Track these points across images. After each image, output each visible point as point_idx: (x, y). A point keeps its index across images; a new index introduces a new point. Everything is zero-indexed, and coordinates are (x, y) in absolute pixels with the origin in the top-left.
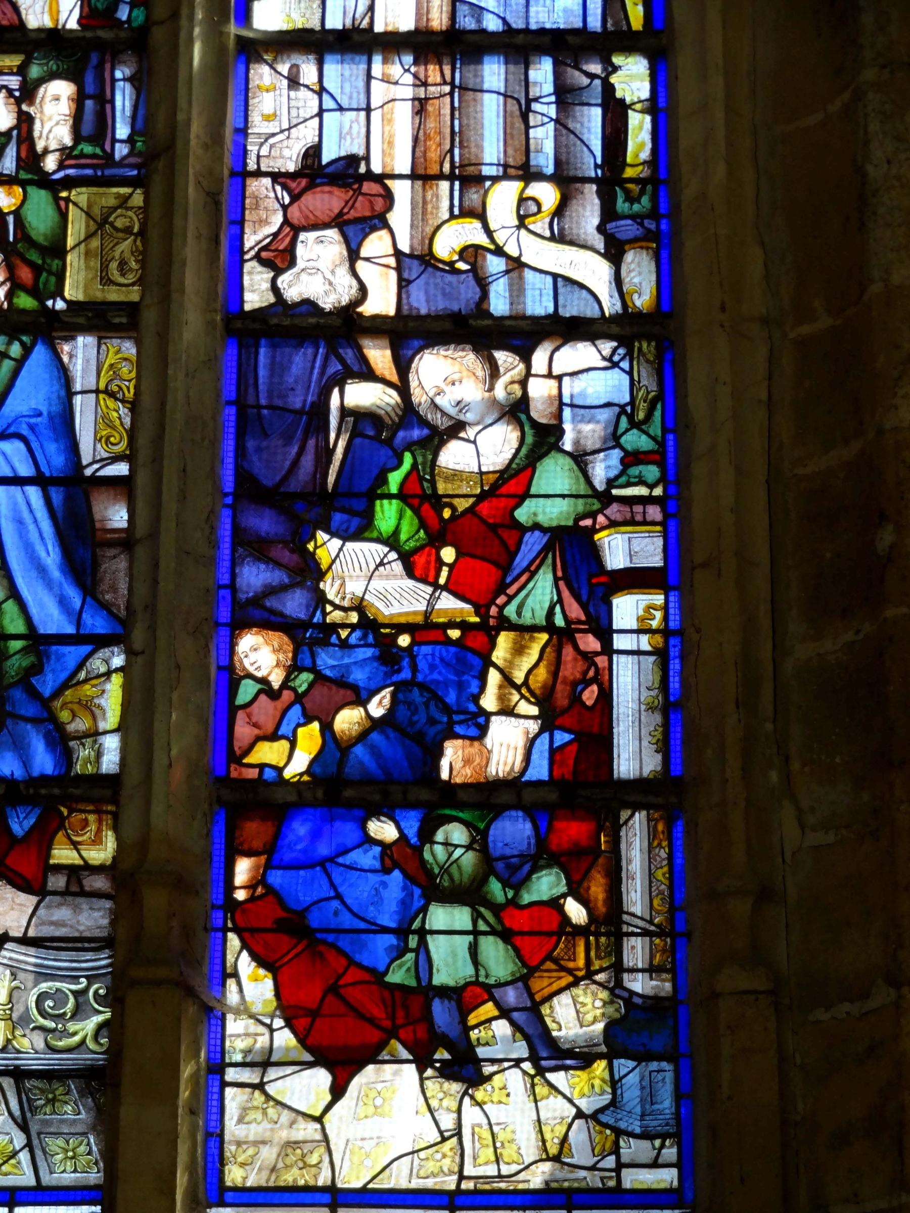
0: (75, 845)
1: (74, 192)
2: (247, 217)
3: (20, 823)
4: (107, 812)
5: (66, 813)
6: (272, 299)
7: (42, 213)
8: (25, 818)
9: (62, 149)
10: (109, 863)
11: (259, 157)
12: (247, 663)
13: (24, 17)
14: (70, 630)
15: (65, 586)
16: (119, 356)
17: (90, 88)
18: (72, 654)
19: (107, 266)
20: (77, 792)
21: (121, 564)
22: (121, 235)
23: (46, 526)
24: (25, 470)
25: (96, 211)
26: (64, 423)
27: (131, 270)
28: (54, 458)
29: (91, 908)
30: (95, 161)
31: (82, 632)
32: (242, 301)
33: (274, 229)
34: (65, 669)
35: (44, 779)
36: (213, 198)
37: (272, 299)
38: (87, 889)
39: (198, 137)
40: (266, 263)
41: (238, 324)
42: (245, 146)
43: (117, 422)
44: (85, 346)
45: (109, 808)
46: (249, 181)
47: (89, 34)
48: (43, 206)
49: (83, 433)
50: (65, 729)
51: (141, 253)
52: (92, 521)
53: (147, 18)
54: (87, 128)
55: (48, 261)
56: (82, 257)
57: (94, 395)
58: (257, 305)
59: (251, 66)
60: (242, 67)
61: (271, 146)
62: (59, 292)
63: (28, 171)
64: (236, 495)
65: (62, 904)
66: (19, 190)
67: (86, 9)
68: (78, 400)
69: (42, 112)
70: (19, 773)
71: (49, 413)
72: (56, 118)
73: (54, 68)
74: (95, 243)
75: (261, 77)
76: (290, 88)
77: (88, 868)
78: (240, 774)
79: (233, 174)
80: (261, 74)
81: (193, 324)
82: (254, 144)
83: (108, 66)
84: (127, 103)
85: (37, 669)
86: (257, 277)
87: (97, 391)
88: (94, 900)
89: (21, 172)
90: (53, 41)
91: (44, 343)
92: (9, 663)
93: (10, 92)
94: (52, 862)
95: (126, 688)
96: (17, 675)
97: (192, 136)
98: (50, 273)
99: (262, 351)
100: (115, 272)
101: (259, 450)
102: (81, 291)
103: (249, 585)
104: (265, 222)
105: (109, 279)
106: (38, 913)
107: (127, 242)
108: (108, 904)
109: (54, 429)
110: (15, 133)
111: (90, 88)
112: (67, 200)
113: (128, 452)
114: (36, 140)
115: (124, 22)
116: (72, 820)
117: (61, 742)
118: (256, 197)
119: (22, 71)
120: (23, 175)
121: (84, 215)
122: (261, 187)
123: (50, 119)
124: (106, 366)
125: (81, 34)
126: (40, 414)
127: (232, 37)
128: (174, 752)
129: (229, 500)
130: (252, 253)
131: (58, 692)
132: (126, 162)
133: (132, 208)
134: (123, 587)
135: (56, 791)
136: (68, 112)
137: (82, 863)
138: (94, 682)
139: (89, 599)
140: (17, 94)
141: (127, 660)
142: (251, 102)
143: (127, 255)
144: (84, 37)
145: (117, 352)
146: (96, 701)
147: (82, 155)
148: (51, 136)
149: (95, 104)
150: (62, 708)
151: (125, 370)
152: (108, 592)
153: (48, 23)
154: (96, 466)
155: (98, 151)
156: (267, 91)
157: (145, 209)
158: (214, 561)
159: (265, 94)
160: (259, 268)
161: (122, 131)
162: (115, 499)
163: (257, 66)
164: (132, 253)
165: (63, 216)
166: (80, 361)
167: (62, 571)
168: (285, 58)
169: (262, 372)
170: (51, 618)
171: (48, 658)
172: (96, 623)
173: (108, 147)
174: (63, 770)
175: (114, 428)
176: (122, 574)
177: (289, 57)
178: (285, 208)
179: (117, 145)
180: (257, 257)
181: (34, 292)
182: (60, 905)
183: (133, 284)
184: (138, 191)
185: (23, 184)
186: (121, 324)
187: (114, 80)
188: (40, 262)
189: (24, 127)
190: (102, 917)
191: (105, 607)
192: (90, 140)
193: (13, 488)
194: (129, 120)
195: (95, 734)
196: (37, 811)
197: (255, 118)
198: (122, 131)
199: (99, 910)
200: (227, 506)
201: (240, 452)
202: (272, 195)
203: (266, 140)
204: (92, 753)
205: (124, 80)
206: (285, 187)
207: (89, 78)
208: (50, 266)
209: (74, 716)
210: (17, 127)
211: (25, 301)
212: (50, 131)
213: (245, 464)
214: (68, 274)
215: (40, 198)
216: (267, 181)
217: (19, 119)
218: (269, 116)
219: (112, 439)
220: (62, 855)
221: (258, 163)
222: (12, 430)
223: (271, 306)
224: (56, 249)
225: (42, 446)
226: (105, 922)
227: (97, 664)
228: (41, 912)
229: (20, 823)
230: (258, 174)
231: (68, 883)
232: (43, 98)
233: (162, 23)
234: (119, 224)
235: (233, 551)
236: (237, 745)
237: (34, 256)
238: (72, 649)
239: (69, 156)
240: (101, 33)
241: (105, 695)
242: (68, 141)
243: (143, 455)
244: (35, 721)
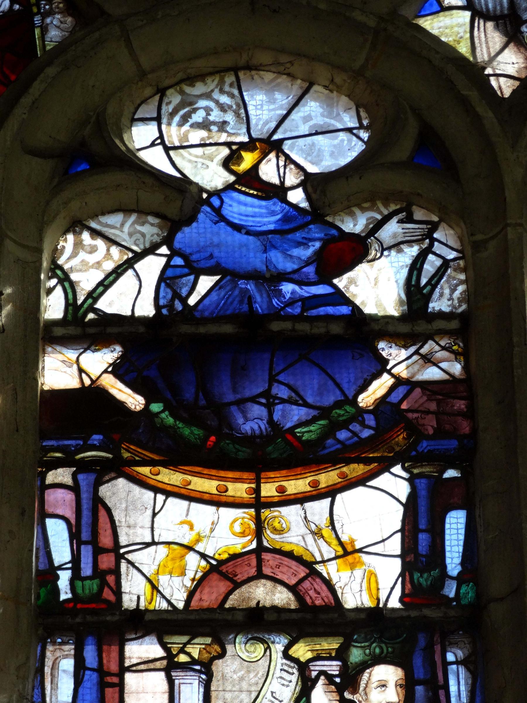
13: (340, 595)
17: (420, 673)
47: (414, 614)
53: (478, 595)
67: (408, 586)
73: (377, 651)
83: (438, 648)
84: (463, 688)
90: (373, 620)
93: (330, 678)
111: (420, 673)
115: (453, 600)
119: (341, 655)
125: (405, 614)
140: (338, 680)
144: (409, 617)
149: (427, 690)
153: (369, 603)
187: (446, 664)
205: (457, 663)
207: (418, 661)
232: (367, 685)
233: (502, 599)
240: (427, 612)
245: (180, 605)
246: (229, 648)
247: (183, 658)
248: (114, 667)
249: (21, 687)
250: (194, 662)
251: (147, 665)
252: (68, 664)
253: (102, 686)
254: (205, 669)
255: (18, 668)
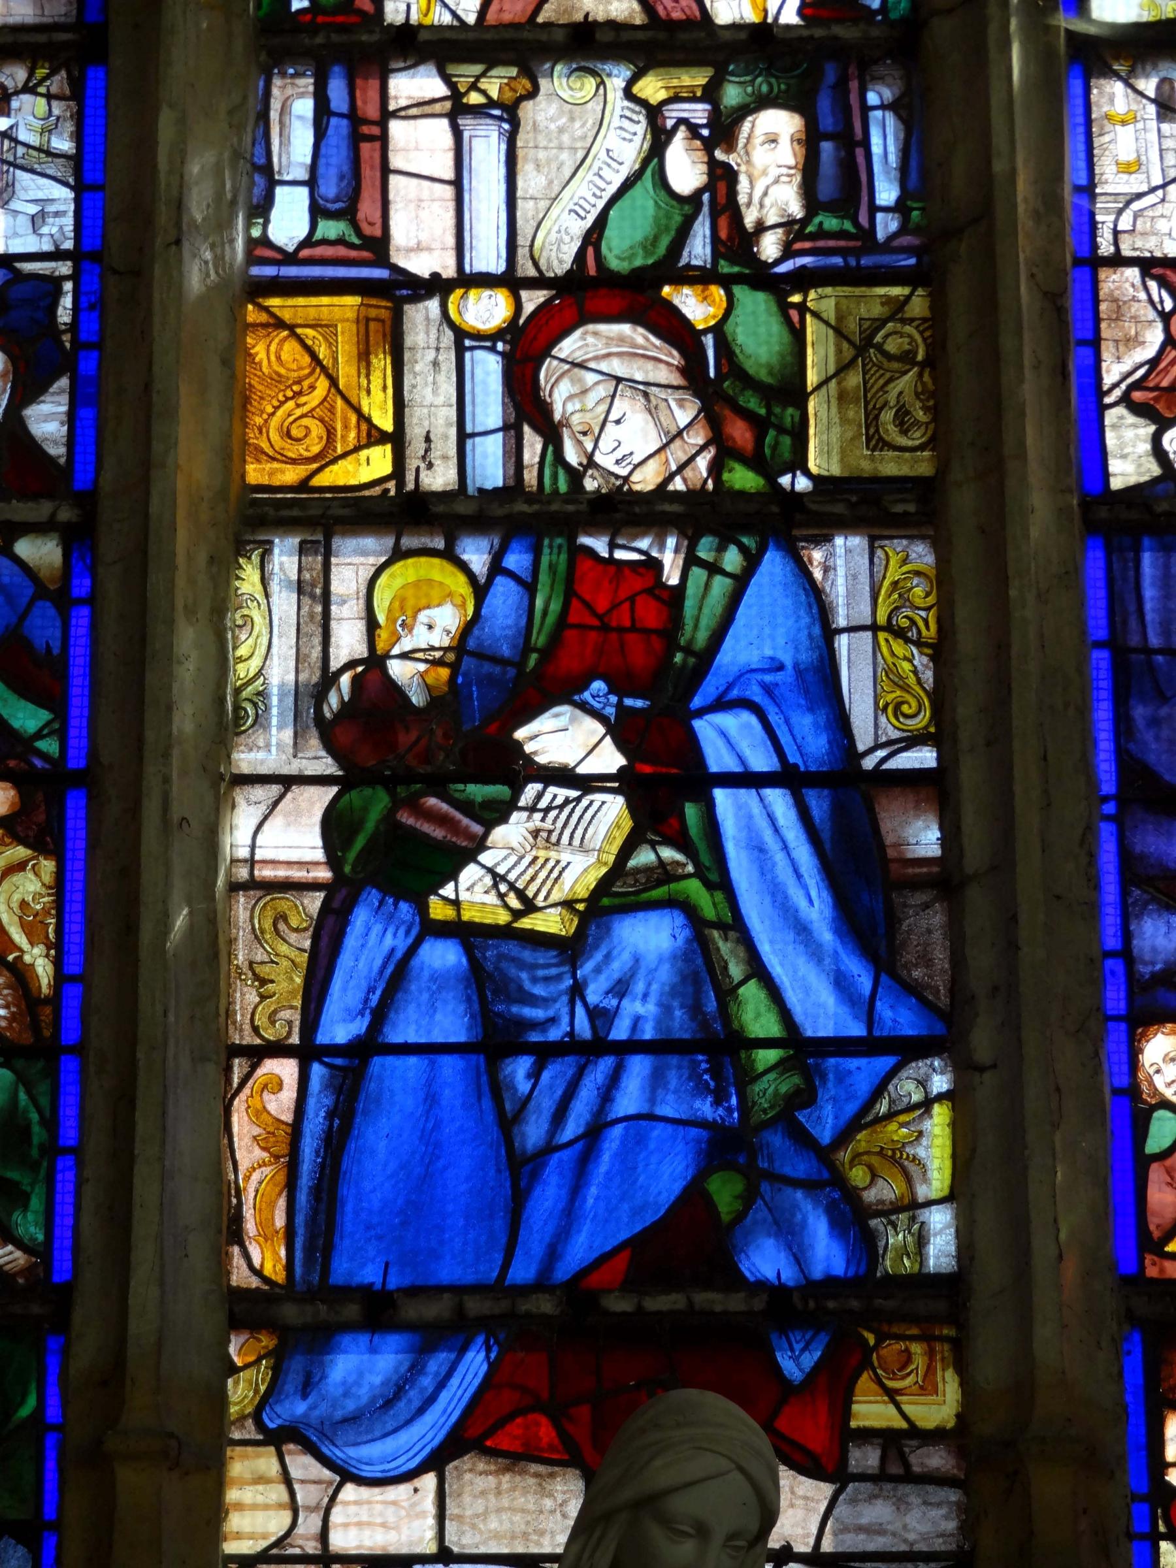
0: (892, 1395)
1: (812, 295)
2: (1104, 335)
3: (796, 1359)
4: (941, 1339)
5: (872, 1342)
6: (1155, 470)
7: (762, 330)
8: (803, 1351)
9: (788, 224)
10: (951, 1424)
11: (1116, 233)
12: (1159, 1082)
14: (857, 1030)
15: (843, 956)
16: (905, 569)
17: (827, 122)
18: (863, 1071)
19: (877, 417)
20: (890, 1304)
21: (936, 918)
22: (895, 365)
23: (804, 854)
24: (761, 761)
25: (852, 326)
26: (822, 682)
27: (917, 423)
28: (810, 741)
29: (925, 1503)
30: (842, 243)
31: (877, 1033)
32: (1106, 475)
33: (1150, 352)
34: (851, 1097)
35: (830, 1281)
36: (1053, 300)
37: (1155, 470)
38: (916, 1469)
39: (1026, 200)
40: (1140, 410)
41: (1103, 513)
42: (1092, 215)
43: (912, 680)
44: (848, 551)
45: (945, 1332)
46: (1103, 273)
47: (819, 32)
48: (763, 317)
49: (855, 697)
50: (860, 1198)
51: (933, 395)
52: (882, 847)
54: (826, 189)
55: (777, 410)
56: (834, 402)
57: (869, 634)
58: (1132, 480)
59: (1093, 82)
60: (1077, 85)
61: (1136, 216)
62: (799, 463)
63: (733, 263)
64: (1119, 798)
65: (876, 1497)
66: (718, 292)
68: (843, 642)
69: (748, 162)
70: (789, 1275)
71: (796, 666)
72: (774, 172)
73: (765, 88)
74: (854, 379)
75: (1112, 101)
76: (1161, 118)
77: (914, 1432)
78: (1162, 1270)
79: (1078, 262)
80: (1111, 97)
81: (1041, 514)
82: (1107, 211)
83: (854, 85)
84: (892, 148)
85: (805, 1097)
86: (1129, 434)
87: (874, 628)
88: (930, 1488)
89: (722, 262)
90: (758, 41)
91: (779, 547)
92: (758, 1087)
93: (694, 130)
94: (853, 1424)
95: (956, 1126)
96: (772, 1107)
97: (1020, 199)
98: (781, 430)
99: (1147, 558)
100: (891, 427)
101: (1154, 722)
102: (835, 458)
103: (1154, 949)
104: (1133, 342)
105: (881, 439)
106: (836, 1512)
107: (907, 378)
108: (954, 1496)
109: (807, 692)
110: (706, 197)
111: (827, 122)
112: (802, 308)
113: (932, 730)
114: (743, 209)
115: (877, 12)
116: (883, 1352)
117: (855, 1220)
118: (1116, 300)
119: (710, 93)
120: (725, 268)
121: (831, 332)
122: (1123, 283)
123: (764, 173)
124: (886, 583)
125: (806, 33)
126: (781, 667)
127: (1062, 33)
128: (1063, 1236)
129: (1110, 808)
130: (1117, 393)
131: (844, 1136)
132: (896, 243)
133: (912, 320)
134: (940, 956)
135: (855, 1304)
136: (792, 162)
137: (904, 1425)
138: (903, 1118)
139: (884, 978)
140: (705, 132)
141: (956, 1081)
142: (1097, 142)
143: (908, 398)
144: (811, 37)
145: (905, 561)
146: (910, 1150)
147: (821, 234)
148: (767, 201)
149: (837, 149)
150: (852, 1164)
151: (919, 591)
152: (916, 966)
153: (751, 16)
154: (881, 753)
155: (848, 226)
156: (1124, 123)
157: (936, 324)
158: (1094, 909)
159: (1118, 128)
160: (1131, 419)
161: (887, 193)
162: (917, 806)
163: (1102, 81)
164: (917, 395)
165: (798, 336)
166: (841, 581)
167: (837, 932)
168: (1148, 68)
169: (1149, 593)
170: (822, 1011)
171: (824, 1077)
172: (899, 1018)
173: (863, 220)
174: (862, 1269)
175: (906, 688)
176: (937, 935)
177: (1155, 66)
178: (1166, 318)
179: (880, 216)
180: (1126, 400)
181: (756, 462)
182: (872, 1497)
183: (921, 448)
184: (920, 291)
185: (727, 282)
186: (906, 514)
187: (866, 109)
188: (763, 411)
189: (722, 187)
190: (946, 1517)
191: (912, 990)
192: (832, 207)
193: (743, 791)
194: (895, 174)
195: (913, 1206)
196: (823, 1339)
197: (1106, 168)
198: (887, 193)
199: (939, 1505)
200: (1108, 818)
201: (1122, 725)
202: (1143, 296)
203: (1128, 203)
204: (909, 1238)
205: (882, 107)
206: (1163, 283)
207: (824, 104)
208: (781, 418)
209: (874, 1176)
210: (708, 187)
211: (742, 478)
212: (765, 194)
213: (1131, 746)
214: (812, 431)
215: (755, 306)
216: (1133, 274)
217: (711, 173)
218: (1129, 164)
219: (905, 708)
220: (871, 1411)
221: (1116, 243)
222: (735, 693)
223: (1155, 481)
224: (789, 389)
225: (787, 722)
226: (951, 1525)
227: (907, 1088)
228: (841, 1509)
229: (796, 1361)
230: (1118, 261)
231: (883, 1459)
232: (749, 139)
234: (891, 346)
235: (1124, 893)
236: (1153, 1224)
237: (752, 403)
238: (862, 1062)
239: (800, 236)
240: (839, 30)
241: (924, 1141)
242: (796, 210)
243: (969, 730)
244: (809, 1186)
245: (471, 19)
246: (543, 83)
247: (475, 98)
248: (372, 112)
249: (235, 140)
250: (491, 103)
251: (422, 109)
252: (304, 107)
253: (356, 139)
254: (508, 113)
255: (230, 113)
